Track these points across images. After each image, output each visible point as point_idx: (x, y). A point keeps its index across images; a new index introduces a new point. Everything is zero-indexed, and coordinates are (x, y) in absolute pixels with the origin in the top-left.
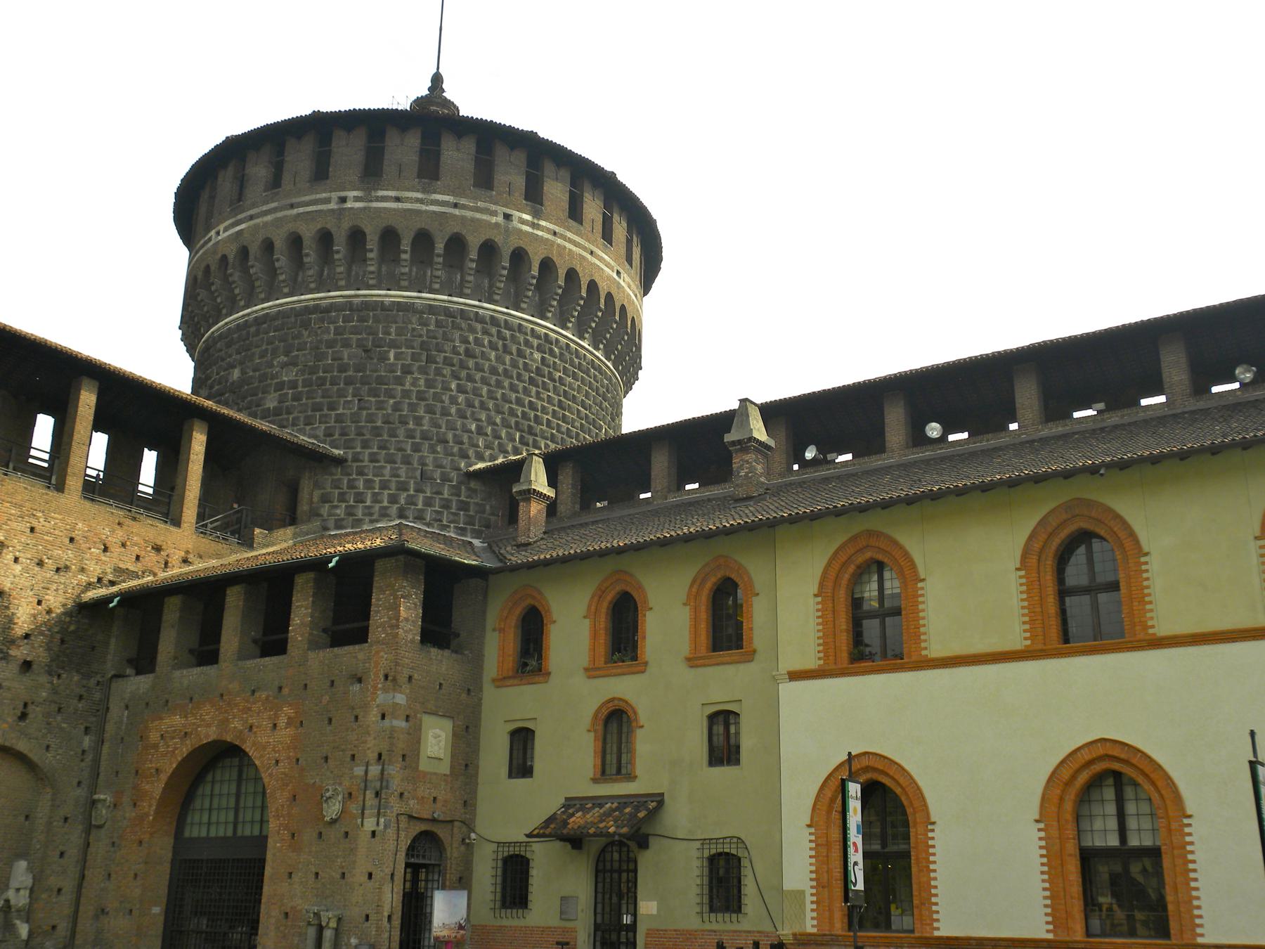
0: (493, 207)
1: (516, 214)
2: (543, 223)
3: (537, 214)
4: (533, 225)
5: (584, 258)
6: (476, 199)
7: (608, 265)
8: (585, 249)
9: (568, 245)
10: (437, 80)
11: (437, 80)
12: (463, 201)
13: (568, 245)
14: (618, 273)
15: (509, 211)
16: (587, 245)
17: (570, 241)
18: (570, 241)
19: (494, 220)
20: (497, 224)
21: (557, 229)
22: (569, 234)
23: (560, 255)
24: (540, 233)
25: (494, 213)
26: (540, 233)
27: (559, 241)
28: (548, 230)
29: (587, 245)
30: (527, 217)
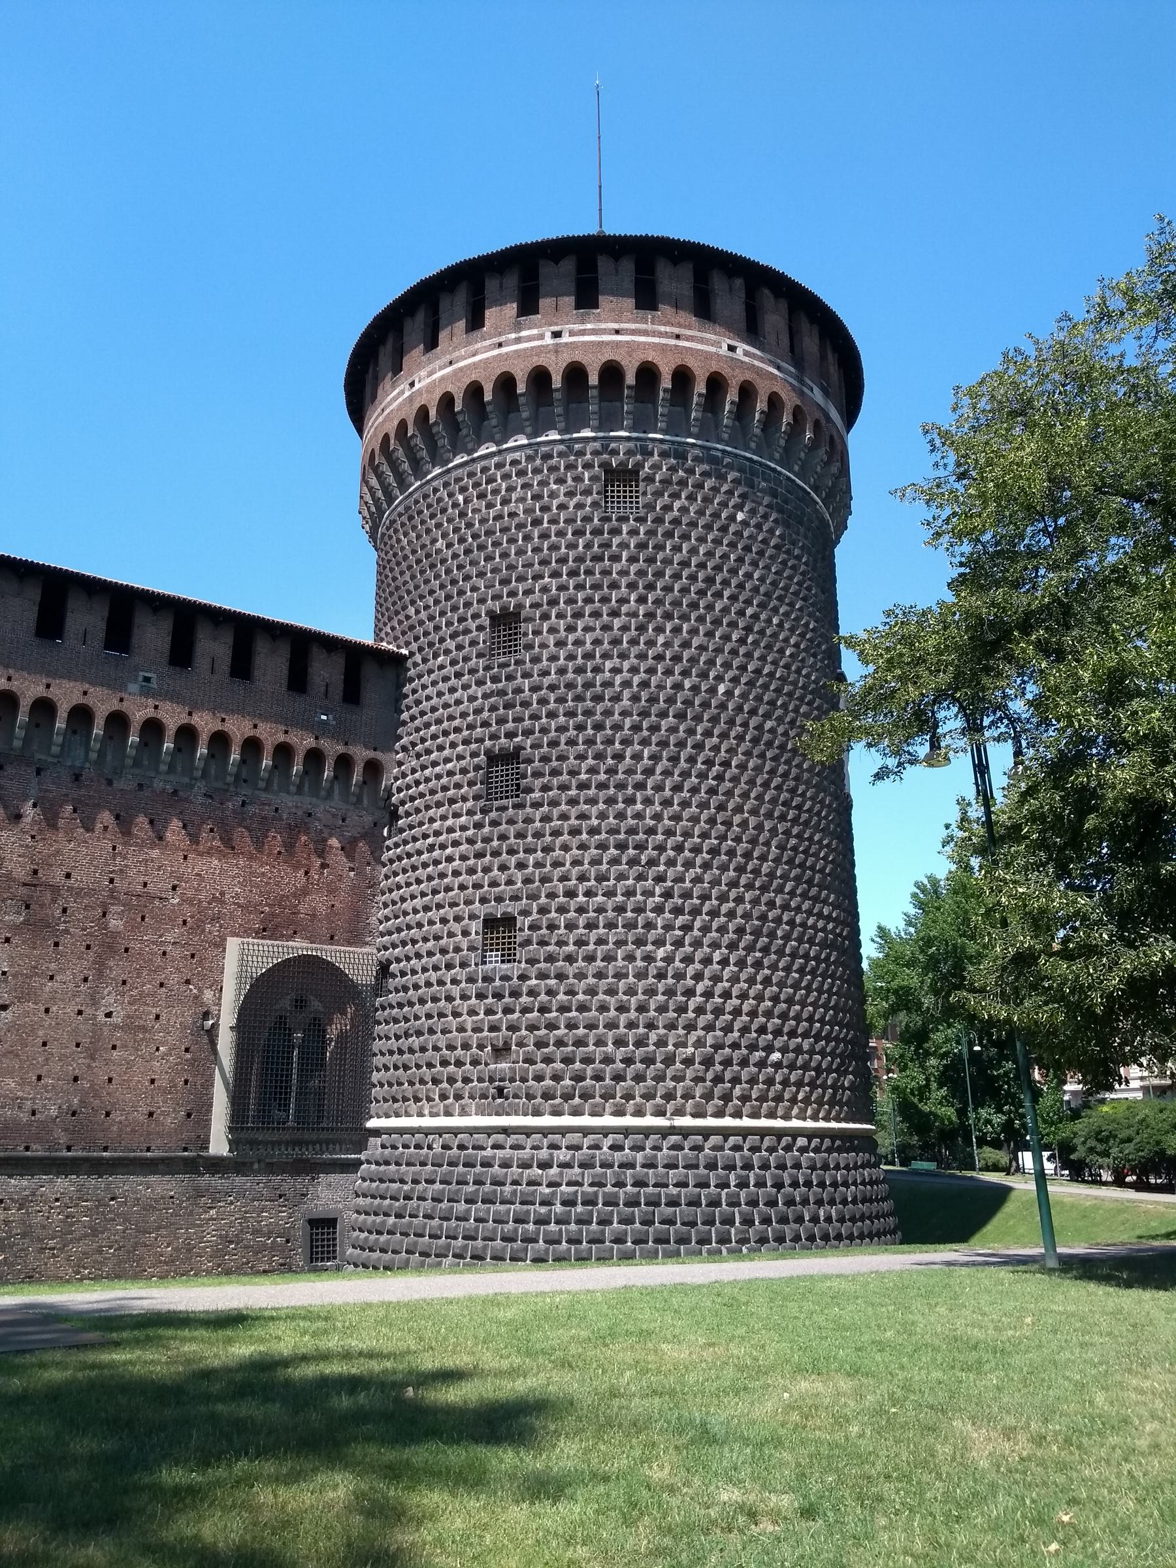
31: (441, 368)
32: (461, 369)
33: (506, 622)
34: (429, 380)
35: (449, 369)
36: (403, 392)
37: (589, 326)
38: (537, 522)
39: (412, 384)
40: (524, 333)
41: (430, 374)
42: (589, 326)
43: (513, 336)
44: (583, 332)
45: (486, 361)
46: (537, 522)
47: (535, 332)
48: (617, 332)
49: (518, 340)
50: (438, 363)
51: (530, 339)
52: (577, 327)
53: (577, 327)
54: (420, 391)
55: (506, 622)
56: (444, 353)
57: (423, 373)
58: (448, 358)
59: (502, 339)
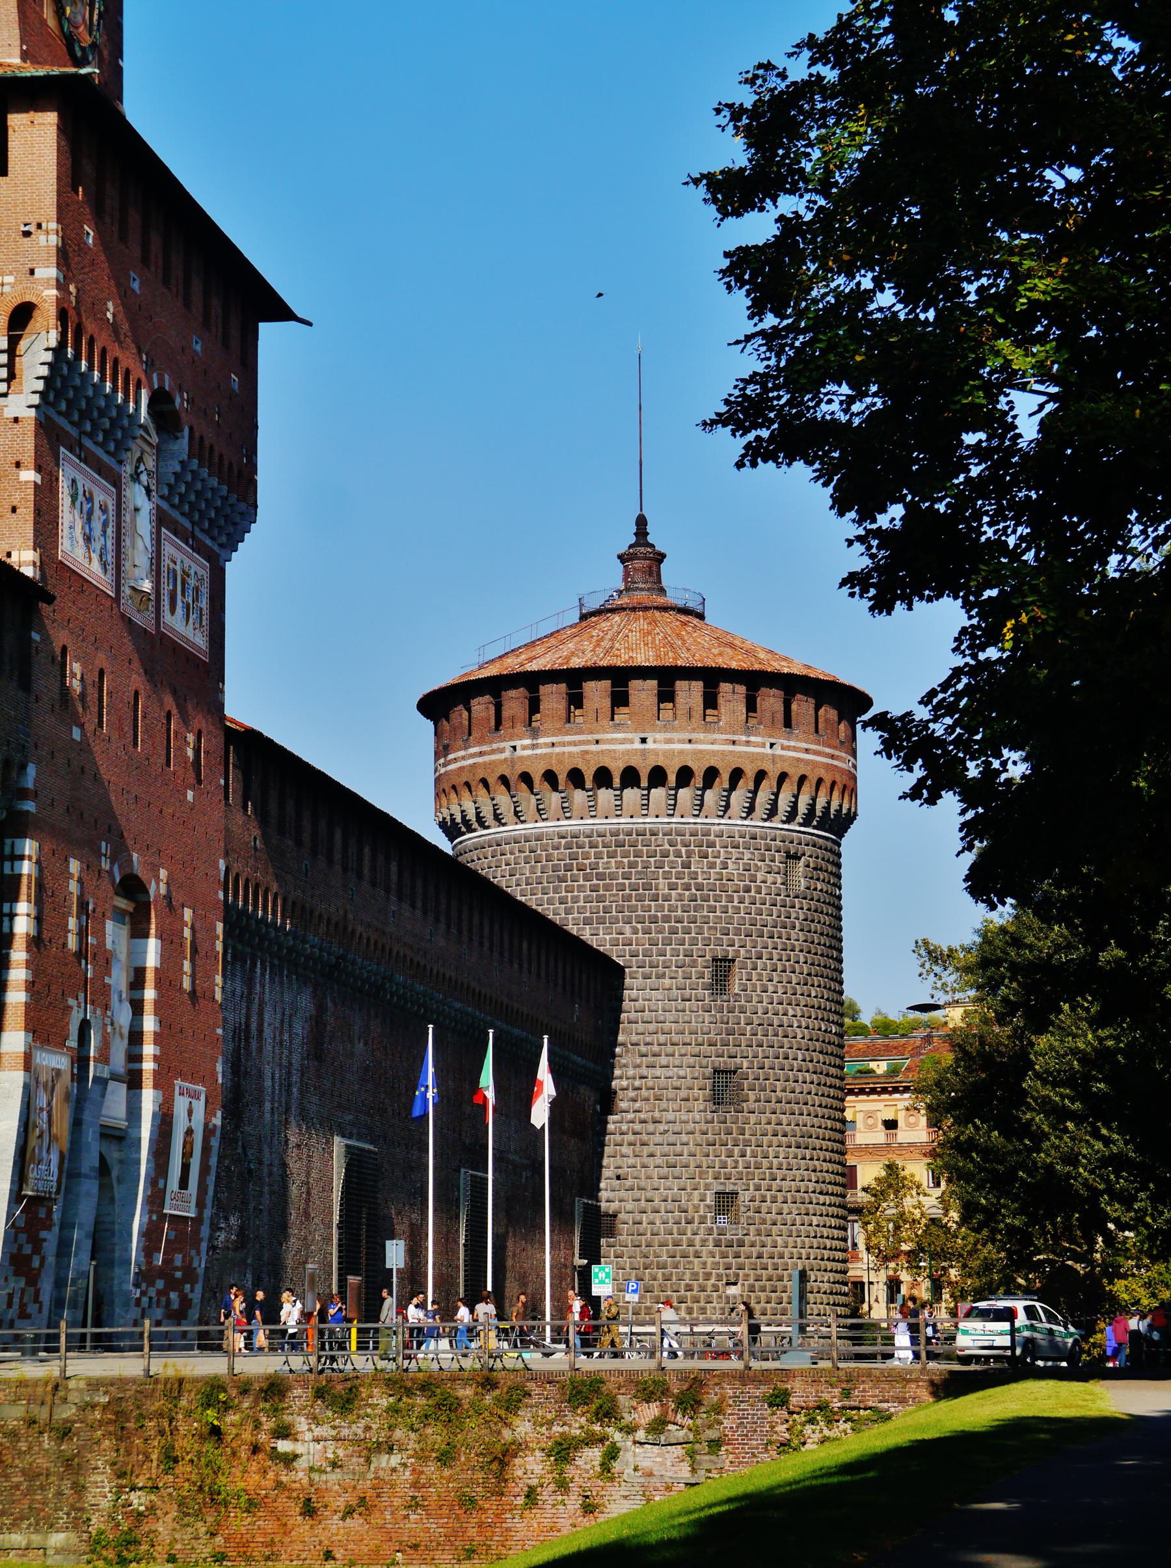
0: (502, 745)
1: (518, 743)
2: (541, 741)
3: (535, 733)
4: (534, 746)
5: (586, 752)
6: (491, 742)
8: (588, 742)
9: (567, 749)
10: (641, 522)
11: (641, 522)
12: (485, 748)
13: (567, 749)
14: (644, 741)
15: (513, 743)
16: (589, 737)
17: (570, 744)
18: (570, 744)
19: (502, 756)
20: (506, 759)
22: (568, 738)
23: (560, 762)
24: (538, 751)
25: (502, 751)
26: (538, 751)
27: (557, 750)
28: (546, 745)
29: (589, 737)
30: (528, 742)
31: (681, 741)
32: (701, 751)
34: (667, 746)
35: (688, 746)
36: (632, 742)
37: (792, 743)
38: (748, 890)
39: (644, 741)
40: (752, 739)
41: (669, 741)
42: (792, 743)
43: (744, 738)
44: (788, 748)
46: (748, 890)
47: (759, 739)
48: (807, 751)
49: (748, 743)
50: (675, 736)
51: (756, 745)
52: (786, 743)
53: (786, 743)
54: (655, 752)
55: (722, 968)
56: (682, 729)
57: (659, 736)
58: (687, 736)
59: (735, 738)
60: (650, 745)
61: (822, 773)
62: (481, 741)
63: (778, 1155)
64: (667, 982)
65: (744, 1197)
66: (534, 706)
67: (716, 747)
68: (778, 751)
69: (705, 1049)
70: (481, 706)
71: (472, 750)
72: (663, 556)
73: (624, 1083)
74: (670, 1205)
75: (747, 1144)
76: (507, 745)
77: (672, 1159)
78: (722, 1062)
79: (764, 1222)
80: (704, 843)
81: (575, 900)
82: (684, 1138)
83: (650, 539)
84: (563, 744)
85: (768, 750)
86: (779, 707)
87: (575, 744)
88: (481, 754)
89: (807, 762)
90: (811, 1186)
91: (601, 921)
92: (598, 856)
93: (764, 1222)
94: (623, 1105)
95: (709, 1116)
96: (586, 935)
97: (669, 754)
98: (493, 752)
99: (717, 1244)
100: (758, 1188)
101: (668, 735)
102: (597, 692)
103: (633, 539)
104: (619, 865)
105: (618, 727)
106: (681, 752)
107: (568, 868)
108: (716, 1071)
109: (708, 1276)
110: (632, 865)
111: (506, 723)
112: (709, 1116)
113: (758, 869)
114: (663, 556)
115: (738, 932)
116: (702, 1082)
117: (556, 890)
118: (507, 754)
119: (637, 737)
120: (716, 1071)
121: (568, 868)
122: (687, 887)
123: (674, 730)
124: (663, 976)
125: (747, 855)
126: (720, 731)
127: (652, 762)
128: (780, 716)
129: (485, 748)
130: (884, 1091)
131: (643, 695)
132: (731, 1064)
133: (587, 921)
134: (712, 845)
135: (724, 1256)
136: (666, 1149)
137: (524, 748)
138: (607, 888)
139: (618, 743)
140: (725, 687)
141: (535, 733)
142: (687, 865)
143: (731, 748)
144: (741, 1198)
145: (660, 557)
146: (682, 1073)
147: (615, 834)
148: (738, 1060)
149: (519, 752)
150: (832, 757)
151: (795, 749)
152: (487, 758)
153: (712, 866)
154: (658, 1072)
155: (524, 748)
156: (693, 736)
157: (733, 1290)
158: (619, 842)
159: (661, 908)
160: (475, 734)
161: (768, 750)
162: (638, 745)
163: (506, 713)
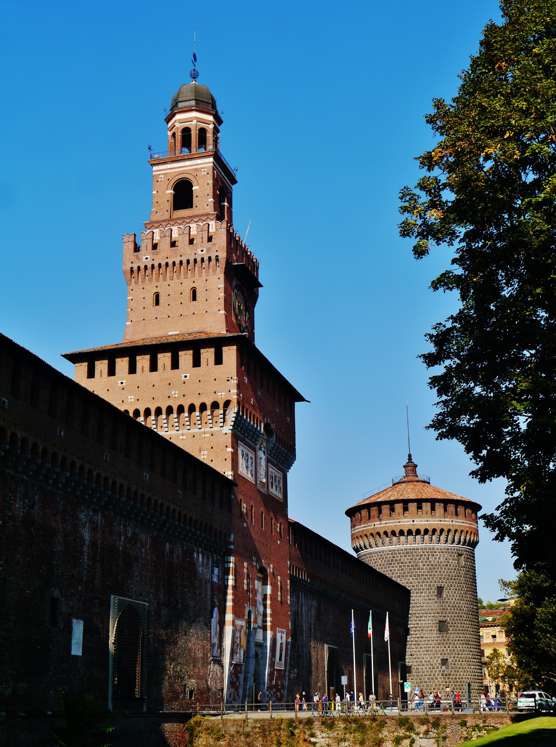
1: (376, 523)
2: (382, 522)
3: (381, 520)
4: (380, 524)
7: (407, 522)
8: (396, 522)
9: (390, 525)
10: (410, 456)
11: (410, 456)
12: (366, 525)
13: (390, 525)
14: (413, 521)
16: (397, 521)
17: (391, 523)
18: (391, 523)
19: (371, 527)
21: (386, 522)
22: (390, 521)
23: (389, 528)
25: (371, 526)
27: (387, 525)
29: (397, 521)
31: (424, 521)
33: (440, 590)
35: (427, 522)
36: (410, 522)
38: (447, 565)
39: (413, 521)
41: (421, 521)
44: (457, 522)
45: (437, 524)
46: (447, 565)
47: (448, 520)
48: (463, 523)
49: (445, 521)
50: (423, 519)
51: (447, 521)
54: (417, 525)
55: (440, 590)
56: (425, 517)
57: (418, 520)
58: (426, 519)
60: (415, 522)
61: (468, 529)
62: (364, 523)
63: (460, 647)
64: (423, 594)
65: (450, 660)
66: (380, 512)
67: (435, 522)
68: (454, 523)
69: (436, 615)
70: (364, 512)
71: (362, 526)
72: (417, 466)
73: (412, 626)
74: (427, 663)
75: (450, 644)
76: (372, 524)
77: (427, 649)
78: (442, 619)
79: (456, 668)
80: (433, 552)
81: (395, 570)
82: (431, 642)
83: (413, 461)
84: (389, 523)
85: (451, 523)
86: (454, 509)
87: (392, 523)
88: (365, 527)
89: (463, 526)
90: (470, 656)
91: (403, 576)
92: (401, 557)
93: (456, 668)
94: (412, 633)
95: (438, 635)
96: (398, 581)
97: (421, 525)
98: (368, 526)
99: (442, 675)
100: (454, 657)
101: (421, 519)
102: (399, 507)
103: (408, 461)
104: (408, 559)
105: (405, 517)
106: (425, 524)
107: (392, 561)
108: (440, 621)
109: (440, 685)
110: (411, 559)
111: (372, 517)
112: (438, 635)
113: (450, 559)
114: (417, 466)
115: (444, 579)
116: (435, 625)
117: (389, 567)
118: (372, 527)
119: (411, 520)
120: (440, 621)
121: (392, 561)
122: (428, 565)
123: (422, 517)
124: (422, 593)
125: (446, 555)
126: (436, 517)
127: (416, 528)
128: (454, 512)
129: (366, 525)
130: (492, 626)
131: (413, 507)
132: (444, 619)
133: (399, 577)
134: (435, 552)
135: (445, 679)
136: (425, 646)
137: (378, 525)
138: (404, 566)
139: (406, 522)
140: (437, 504)
141: (381, 520)
142: (428, 559)
143: (440, 522)
144: (449, 660)
145: (416, 466)
146: (429, 622)
147: (406, 550)
148: (446, 618)
149: (376, 526)
150: (471, 524)
151: (459, 522)
152: (366, 528)
153: (436, 558)
154: (422, 622)
155: (378, 525)
156: (428, 519)
157: (448, 689)
158: (407, 552)
159: (421, 572)
160: (363, 521)
161: (451, 523)
162: (412, 523)
163: (372, 514)
